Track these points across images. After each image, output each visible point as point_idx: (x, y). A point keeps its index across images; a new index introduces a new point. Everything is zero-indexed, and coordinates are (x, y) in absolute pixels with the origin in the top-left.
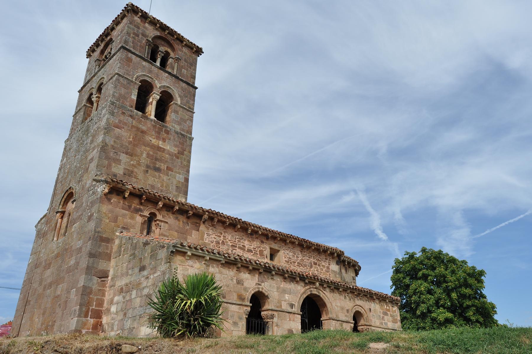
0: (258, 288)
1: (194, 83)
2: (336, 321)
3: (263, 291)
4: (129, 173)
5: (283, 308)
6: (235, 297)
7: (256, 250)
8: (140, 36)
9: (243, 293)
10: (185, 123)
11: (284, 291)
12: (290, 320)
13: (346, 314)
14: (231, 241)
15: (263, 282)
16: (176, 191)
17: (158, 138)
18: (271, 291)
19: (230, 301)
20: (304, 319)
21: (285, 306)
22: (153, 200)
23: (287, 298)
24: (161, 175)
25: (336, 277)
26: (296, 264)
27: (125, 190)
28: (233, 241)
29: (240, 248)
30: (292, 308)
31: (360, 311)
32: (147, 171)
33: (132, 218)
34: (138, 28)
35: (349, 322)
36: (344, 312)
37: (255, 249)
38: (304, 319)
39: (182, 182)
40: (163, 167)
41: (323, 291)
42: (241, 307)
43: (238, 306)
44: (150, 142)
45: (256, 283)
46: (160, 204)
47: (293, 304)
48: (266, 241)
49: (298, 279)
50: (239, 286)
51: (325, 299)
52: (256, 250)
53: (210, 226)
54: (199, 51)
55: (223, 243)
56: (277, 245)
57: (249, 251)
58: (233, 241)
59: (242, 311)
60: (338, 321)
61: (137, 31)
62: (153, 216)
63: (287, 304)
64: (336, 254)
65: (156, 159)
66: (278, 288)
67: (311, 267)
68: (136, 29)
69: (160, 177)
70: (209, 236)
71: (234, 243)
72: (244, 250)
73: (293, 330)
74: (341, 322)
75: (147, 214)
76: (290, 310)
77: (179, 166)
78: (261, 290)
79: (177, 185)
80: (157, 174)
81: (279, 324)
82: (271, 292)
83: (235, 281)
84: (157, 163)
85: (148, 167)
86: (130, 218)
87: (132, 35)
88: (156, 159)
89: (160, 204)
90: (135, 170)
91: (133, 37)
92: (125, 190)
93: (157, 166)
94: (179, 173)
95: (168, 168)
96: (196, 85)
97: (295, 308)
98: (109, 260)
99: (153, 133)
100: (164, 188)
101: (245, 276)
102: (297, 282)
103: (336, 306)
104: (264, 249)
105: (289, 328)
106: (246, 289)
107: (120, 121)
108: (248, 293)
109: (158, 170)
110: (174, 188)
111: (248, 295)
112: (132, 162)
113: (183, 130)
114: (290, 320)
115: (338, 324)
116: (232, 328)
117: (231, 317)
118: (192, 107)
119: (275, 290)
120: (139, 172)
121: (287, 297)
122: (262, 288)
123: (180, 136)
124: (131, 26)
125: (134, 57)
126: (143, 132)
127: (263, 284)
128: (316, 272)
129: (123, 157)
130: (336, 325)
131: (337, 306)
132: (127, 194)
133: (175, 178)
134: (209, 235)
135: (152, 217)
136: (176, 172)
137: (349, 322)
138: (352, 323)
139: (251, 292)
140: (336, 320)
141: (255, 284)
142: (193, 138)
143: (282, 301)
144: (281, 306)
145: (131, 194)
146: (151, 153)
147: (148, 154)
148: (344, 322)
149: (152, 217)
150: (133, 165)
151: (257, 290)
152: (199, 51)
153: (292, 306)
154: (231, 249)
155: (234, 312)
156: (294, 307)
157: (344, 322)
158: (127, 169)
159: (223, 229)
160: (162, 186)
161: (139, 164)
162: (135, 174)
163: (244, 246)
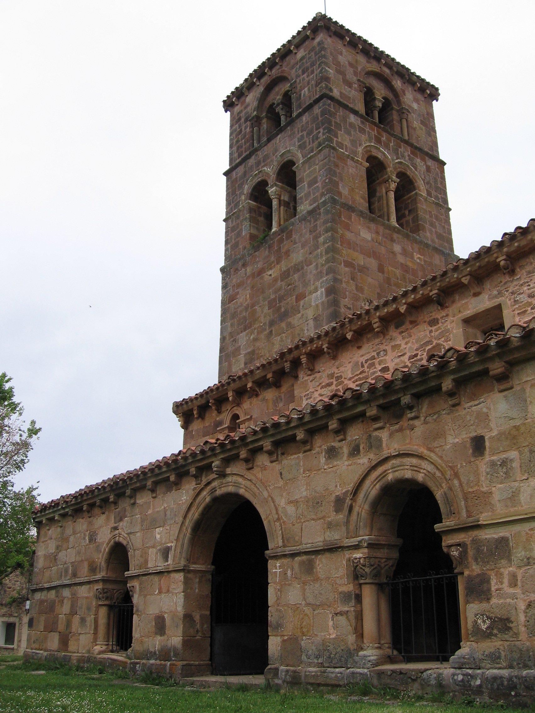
2: (285, 561)
7: (419, 357)
13: (333, 517)
14: (353, 377)
27: (193, 408)
28: (357, 375)
31: (408, 475)
32: (271, 332)
35: (342, 548)
37: (416, 355)
44: (270, 278)
48: (443, 313)
52: (419, 357)
53: (310, 375)
56: (485, 297)
58: (357, 375)
60: (293, 555)
69: (289, 325)
70: (311, 398)
71: (360, 379)
74: (304, 557)
79: (315, 316)
92: (193, 408)
94: (316, 290)
103: (291, 502)
104: (443, 339)
112: (252, 337)
115: (296, 566)
131: (295, 503)
133: (310, 306)
134: (309, 396)
136: (311, 293)
137: (342, 548)
138: (357, 547)
140: (285, 556)
148: (317, 552)
157: (317, 552)
159: (333, 362)
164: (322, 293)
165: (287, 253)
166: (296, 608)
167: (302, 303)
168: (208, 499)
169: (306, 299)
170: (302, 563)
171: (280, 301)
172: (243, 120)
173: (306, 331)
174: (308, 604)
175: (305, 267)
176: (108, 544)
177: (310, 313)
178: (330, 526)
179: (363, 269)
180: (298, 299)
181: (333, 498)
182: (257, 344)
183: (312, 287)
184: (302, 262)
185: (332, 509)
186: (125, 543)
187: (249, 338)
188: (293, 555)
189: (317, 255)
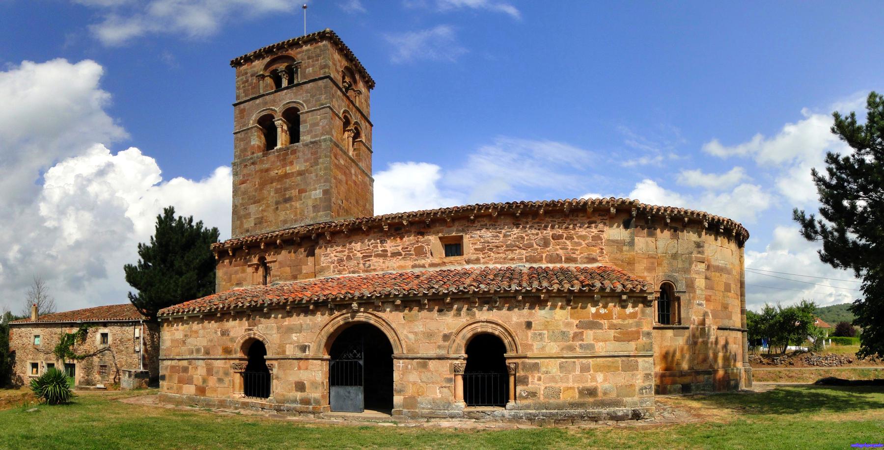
0: (249, 334)
2: (407, 361)
3: (256, 337)
4: (260, 222)
5: (287, 353)
6: (220, 350)
9: (230, 345)
11: (290, 330)
12: (299, 368)
13: (441, 343)
15: (255, 325)
16: (314, 212)
18: (267, 334)
19: (212, 357)
20: (356, 360)
21: (290, 351)
23: (295, 339)
24: (293, 203)
30: (304, 351)
32: (277, 208)
36: (435, 341)
38: (356, 360)
39: (320, 198)
40: (294, 192)
41: (375, 312)
42: (227, 361)
43: (224, 361)
45: (246, 329)
47: (306, 346)
50: (224, 338)
51: (382, 325)
59: (228, 366)
60: (413, 359)
63: (294, 347)
66: (278, 328)
69: (291, 206)
73: (305, 382)
76: (299, 354)
77: (314, 180)
78: (252, 336)
80: (288, 205)
81: (279, 376)
82: (268, 336)
83: (219, 333)
88: (286, 189)
90: (265, 214)
93: (287, 196)
94: (315, 189)
97: (309, 350)
100: (299, 216)
105: (297, 379)
106: (232, 340)
108: (235, 344)
109: (287, 200)
110: (311, 209)
111: (237, 346)
114: (299, 368)
116: (217, 385)
117: (216, 373)
119: (275, 331)
120: (270, 215)
121: (294, 337)
122: (255, 334)
123: (311, 146)
127: (256, 328)
130: (407, 367)
131: (416, 334)
133: (310, 198)
135: (263, 263)
136: (311, 190)
139: (239, 341)
140: (407, 358)
141: (243, 331)
143: (286, 344)
144: (284, 352)
146: (279, 186)
148: (430, 359)
150: (262, 210)
151: (247, 337)
153: (304, 348)
155: (219, 367)
156: (307, 350)
157: (430, 359)
158: (257, 218)
160: (296, 215)
161: (268, 206)
162: (265, 218)
164: (320, 192)
166: (414, 383)
167: (303, 195)
168: (342, 323)
169: (307, 193)
170: (417, 363)
171: (285, 191)
173: (306, 212)
174: (422, 382)
175: (307, 174)
176: (242, 338)
177: (310, 203)
178: (439, 347)
179: (340, 181)
180: (301, 192)
181: (442, 334)
182: (265, 214)
183: (312, 187)
184: (304, 170)
185: (441, 339)
186: (261, 339)
187: (259, 209)
188: (413, 359)
189: (317, 169)
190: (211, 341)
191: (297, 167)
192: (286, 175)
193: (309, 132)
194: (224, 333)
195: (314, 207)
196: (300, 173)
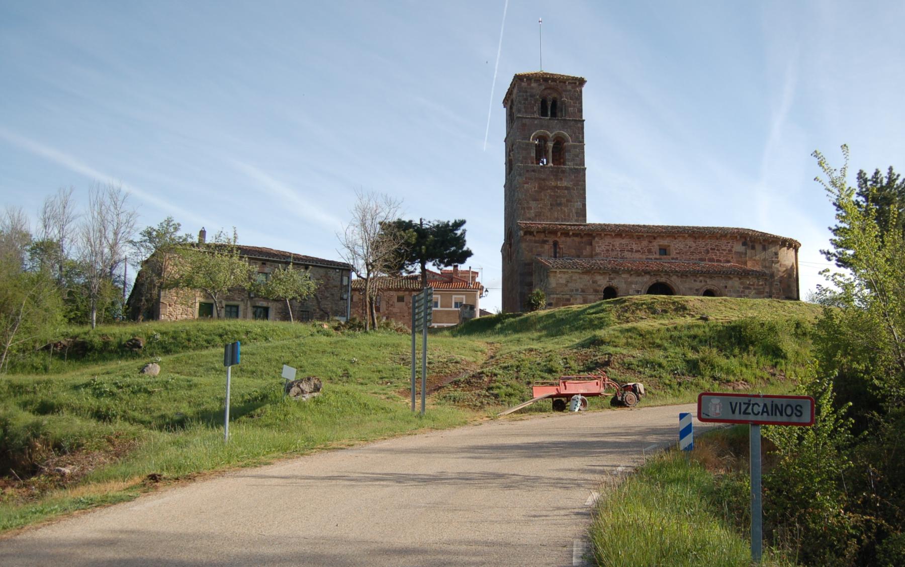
1: (581, 116)
6: (592, 290)
8: (529, 99)
10: (578, 157)
17: (556, 180)
22: (553, 232)
24: (563, 208)
25: (741, 257)
26: (689, 253)
29: (627, 251)
32: (552, 209)
33: (542, 247)
34: (527, 92)
40: (564, 200)
46: (559, 234)
49: (643, 274)
54: (582, 82)
55: (612, 250)
57: (637, 251)
61: (526, 95)
62: (555, 244)
64: (738, 237)
65: (558, 197)
66: (625, 282)
67: (708, 252)
68: (524, 94)
69: (561, 209)
72: (632, 252)
75: (551, 243)
83: (591, 282)
84: (558, 199)
85: (551, 205)
86: (541, 248)
87: (523, 102)
88: (558, 197)
89: (559, 234)
91: (524, 103)
93: (559, 202)
94: (577, 202)
95: (568, 201)
96: (583, 119)
98: (532, 275)
99: (552, 177)
101: (598, 278)
102: (642, 276)
106: (600, 286)
107: (526, 178)
109: (560, 204)
113: (577, 165)
118: (581, 140)
119: (623, 283)
121: (633, 286)
124: (521, 94)
125: (527, 120)
126: (544, 180)
128: (714, 257)
129: (533, 204)
131: (685, 288)
132: (535, 234)
133: (574, 207)
142: (586, 168)
145: (537, 232)
146: (552, 194)
147: (550, 195)
149: (555, 244)
151: (608, 285)
152: (582, 82)
154: (619, 253)
163: (632, 249)
165: (561, 179)
167: (569, 204)
172: (528, 94)
180: (568, 201)
190: (586, 285)
191: (565, 184)
192: (557, 187)
193: (573, 160)
194: (594, 282)
195: (576, 213)
196: (567, 188)
